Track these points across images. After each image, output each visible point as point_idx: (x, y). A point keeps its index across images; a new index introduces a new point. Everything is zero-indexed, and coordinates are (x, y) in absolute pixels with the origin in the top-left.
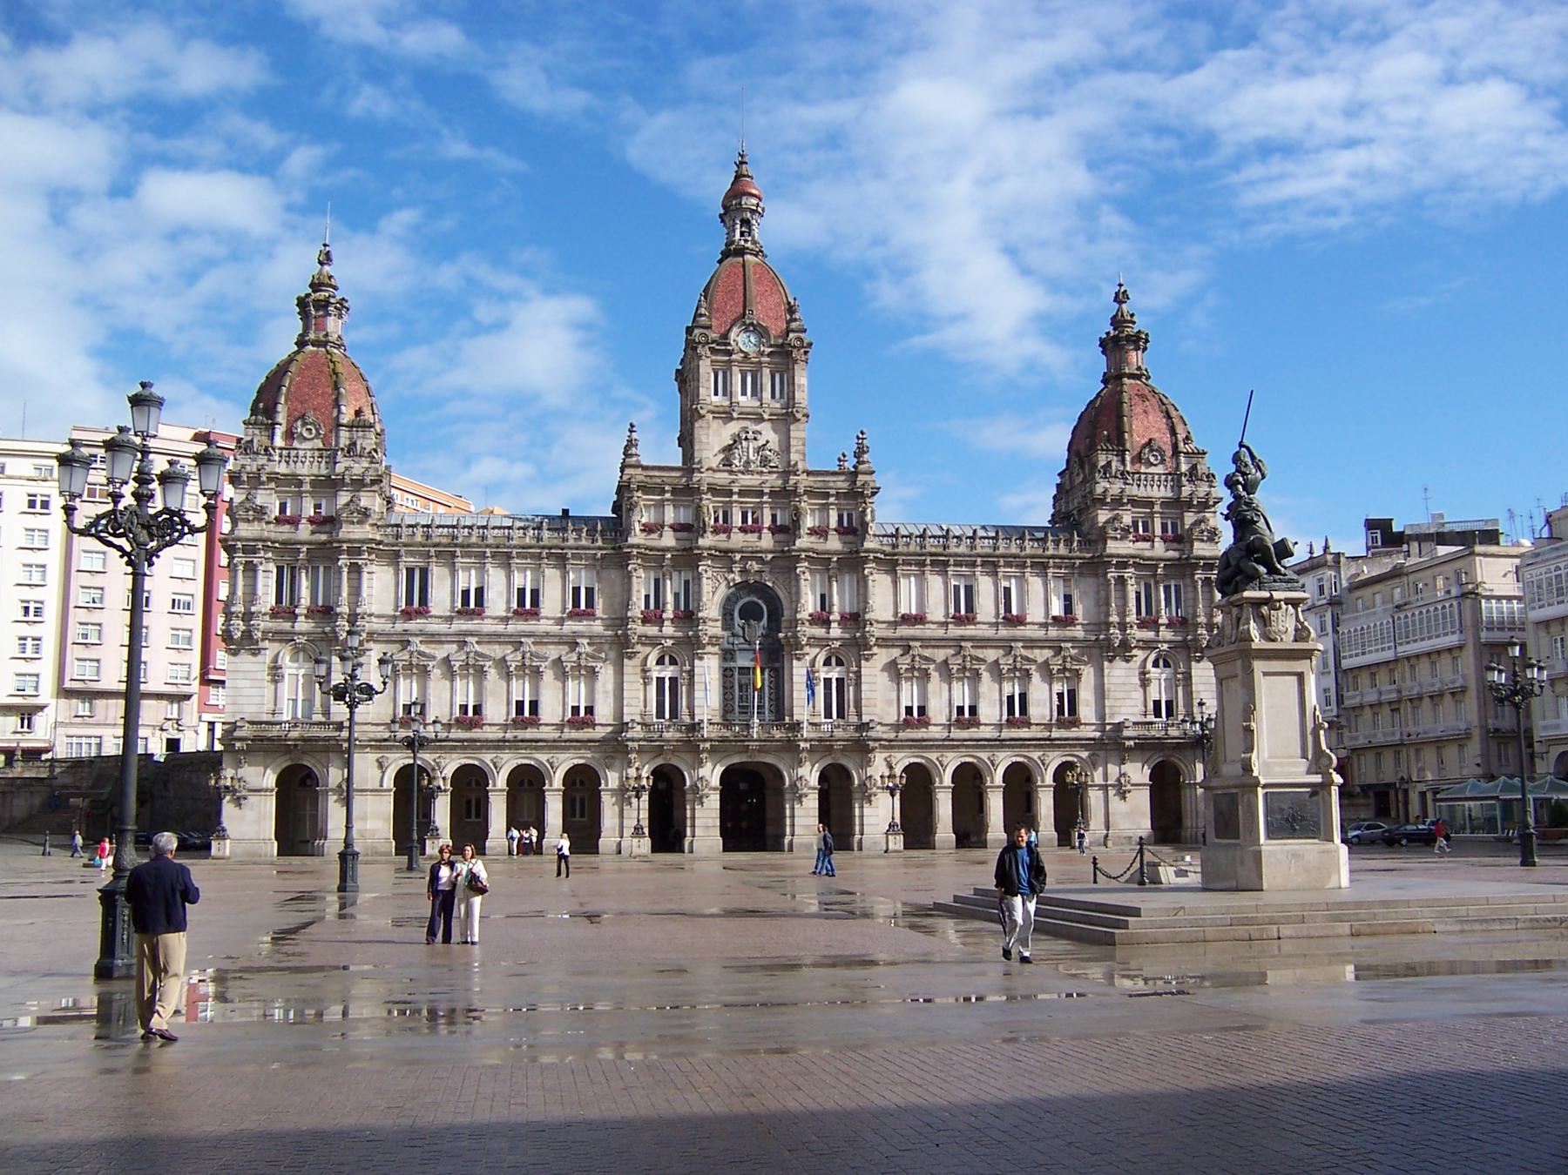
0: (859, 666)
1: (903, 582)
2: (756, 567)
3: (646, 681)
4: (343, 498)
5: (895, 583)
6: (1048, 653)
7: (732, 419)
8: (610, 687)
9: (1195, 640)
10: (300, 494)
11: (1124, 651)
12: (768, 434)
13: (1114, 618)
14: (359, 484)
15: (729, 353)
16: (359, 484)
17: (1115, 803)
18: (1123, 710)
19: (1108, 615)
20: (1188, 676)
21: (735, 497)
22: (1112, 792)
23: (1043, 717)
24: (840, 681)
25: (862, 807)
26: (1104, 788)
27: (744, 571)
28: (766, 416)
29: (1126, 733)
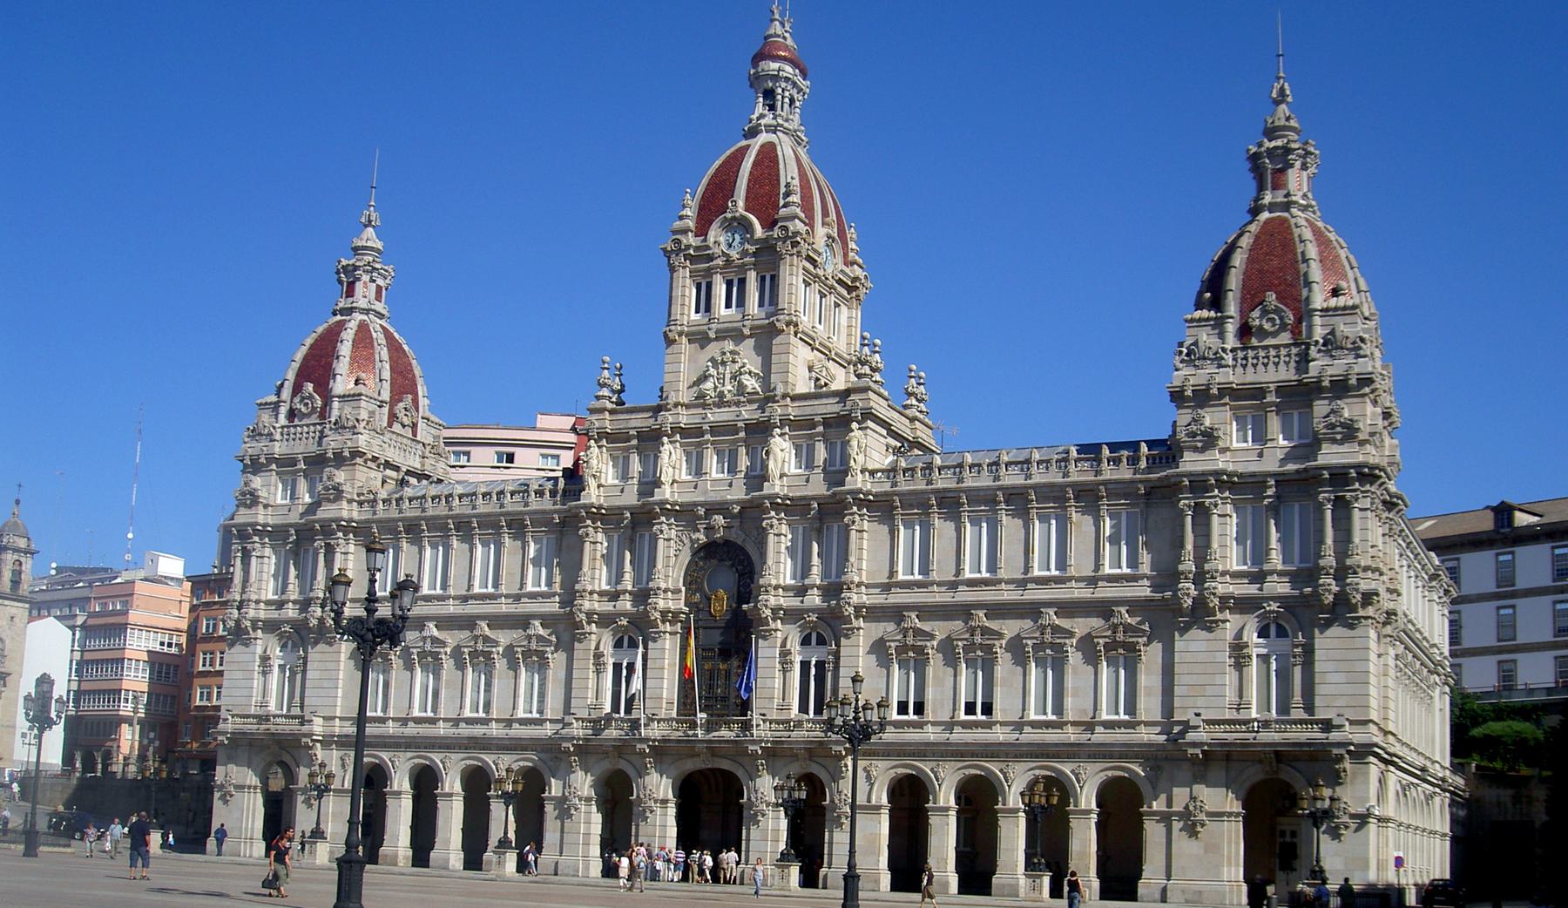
0: (838, 645)
1: (428, 552)
2: (719, 520)
3: (599, 668)
4: (1320, 407)
5: (959, 531)
6: (1096, 623)
7: (709, 340)
8: (562, 674)
9: (1316, 595)
10: (1264, 408)
11: (1201, 615)
12: (748, 358)
13: (1188, 565)
14: (1341, 388)
15: (711, 258)
16: (1341, 388)
17: (1181, 842)
18: (1200, 702)
19: (1178, 560)
20: (1309, 651)
21: (707, 437)
22: (1177, 825)
23: (1085, 711)
24: (820, 665)
25: (831, 832)
26: (1166, 818)
27: (710, 529)
28: (747, 332)
29: (1191, 736)
